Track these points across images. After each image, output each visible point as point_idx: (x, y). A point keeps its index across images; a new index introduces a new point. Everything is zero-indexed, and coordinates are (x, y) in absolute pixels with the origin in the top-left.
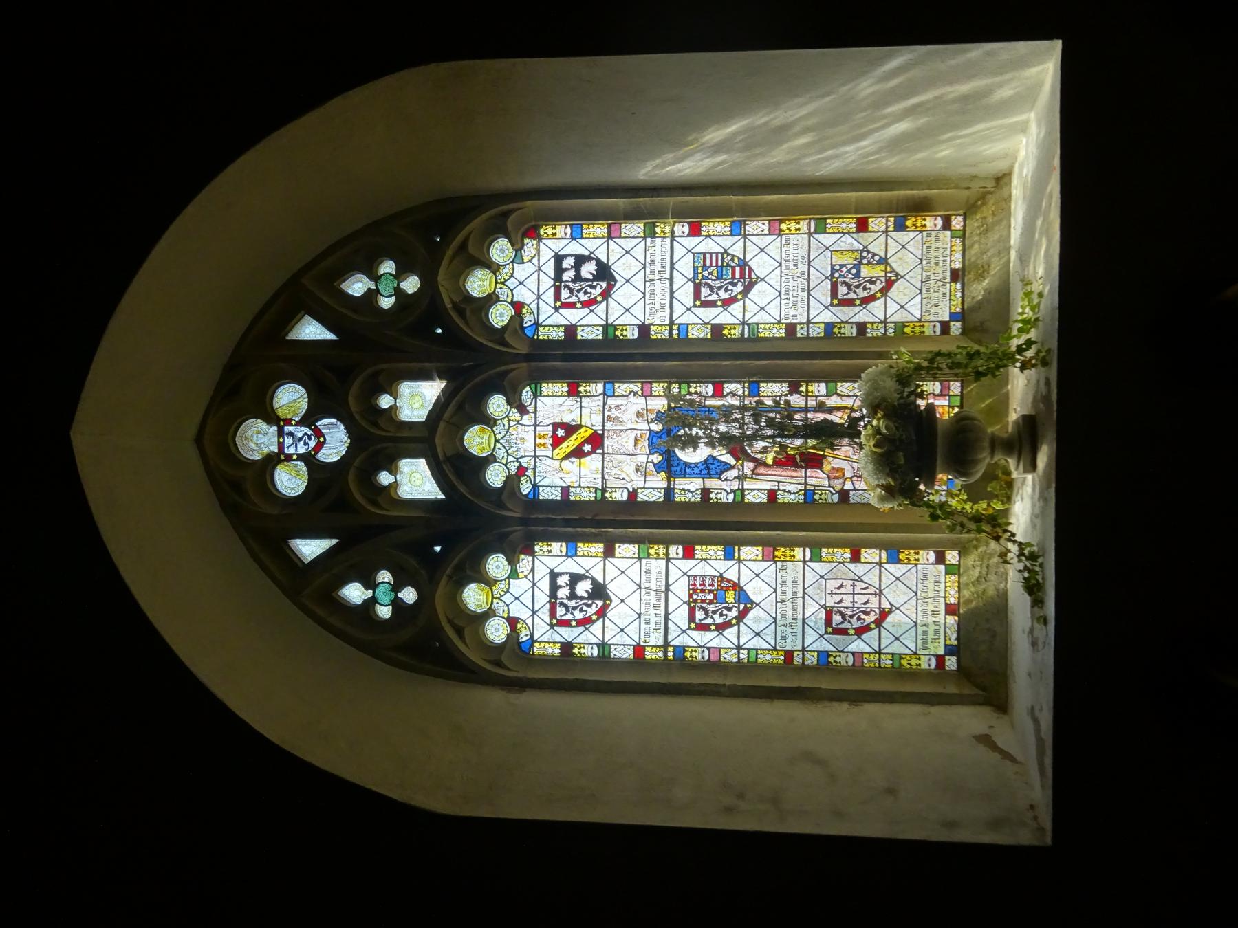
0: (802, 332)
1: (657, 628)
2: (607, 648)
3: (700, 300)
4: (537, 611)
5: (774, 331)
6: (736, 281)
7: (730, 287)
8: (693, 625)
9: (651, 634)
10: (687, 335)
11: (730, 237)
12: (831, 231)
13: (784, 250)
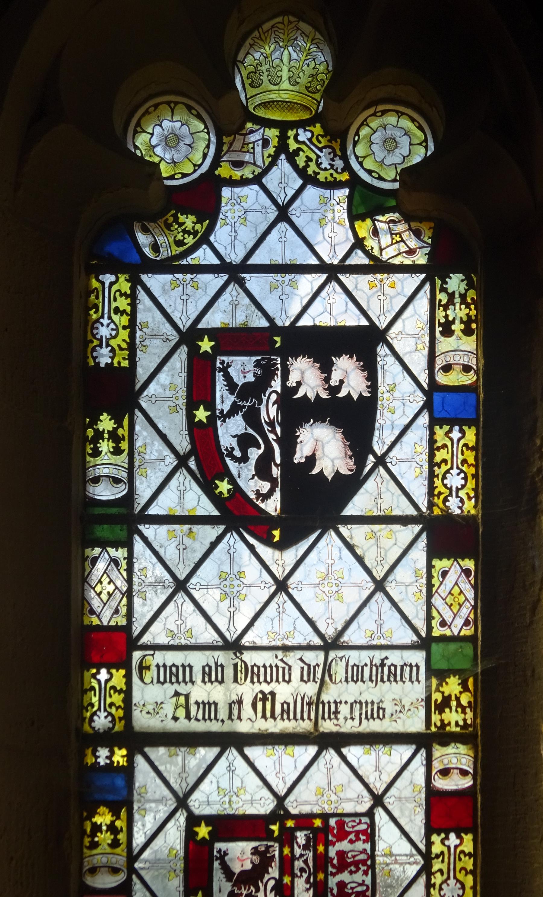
1: (193, 709)
2: (120, 532)
4: (241, 284)
8: (203, 831)
9: (170, 689)
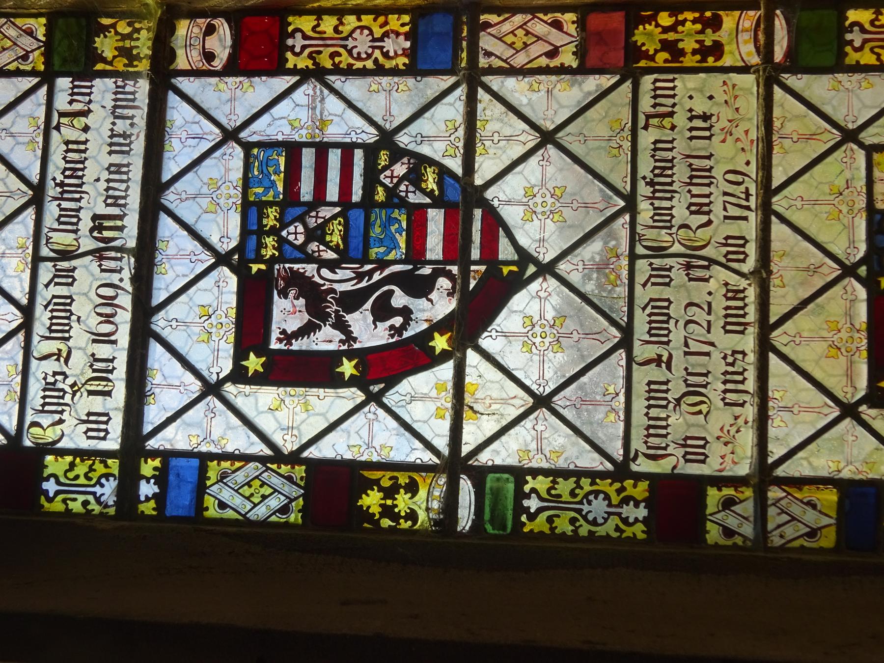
0: (732, 522)
3: (262, 349)
5: (598, 507)
6: (427, 270)
7: (399, 299)
10: (200, 507)
11: (411, 81)
12: (867, 58)
13: (646, 139)
